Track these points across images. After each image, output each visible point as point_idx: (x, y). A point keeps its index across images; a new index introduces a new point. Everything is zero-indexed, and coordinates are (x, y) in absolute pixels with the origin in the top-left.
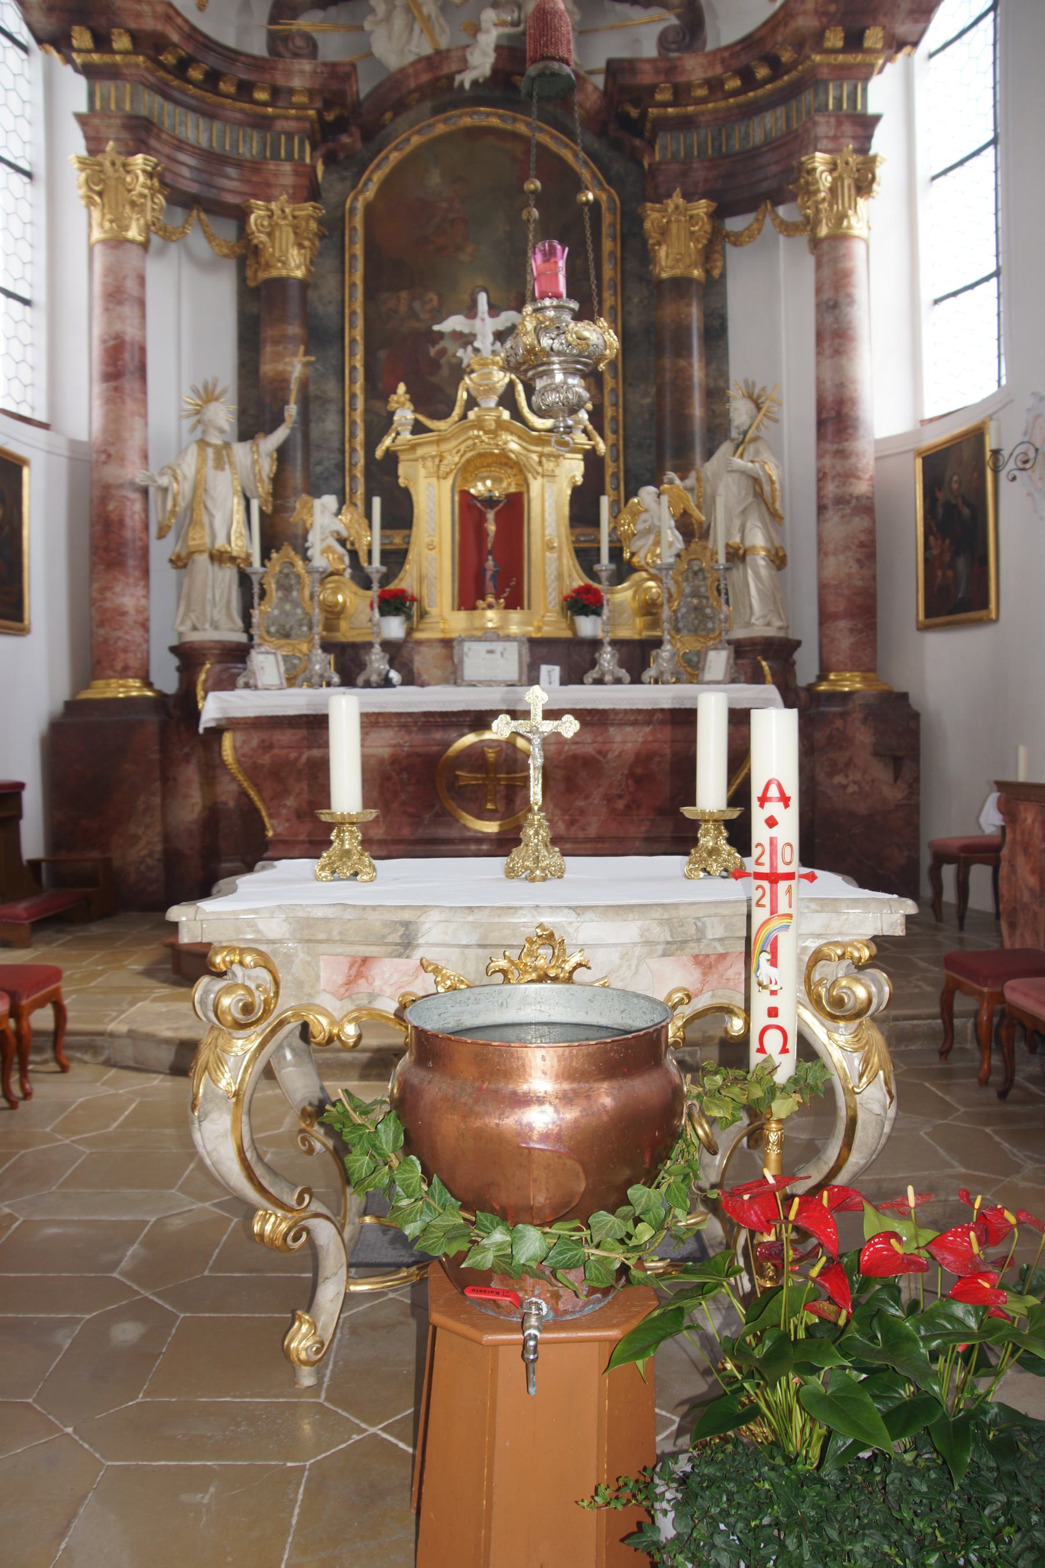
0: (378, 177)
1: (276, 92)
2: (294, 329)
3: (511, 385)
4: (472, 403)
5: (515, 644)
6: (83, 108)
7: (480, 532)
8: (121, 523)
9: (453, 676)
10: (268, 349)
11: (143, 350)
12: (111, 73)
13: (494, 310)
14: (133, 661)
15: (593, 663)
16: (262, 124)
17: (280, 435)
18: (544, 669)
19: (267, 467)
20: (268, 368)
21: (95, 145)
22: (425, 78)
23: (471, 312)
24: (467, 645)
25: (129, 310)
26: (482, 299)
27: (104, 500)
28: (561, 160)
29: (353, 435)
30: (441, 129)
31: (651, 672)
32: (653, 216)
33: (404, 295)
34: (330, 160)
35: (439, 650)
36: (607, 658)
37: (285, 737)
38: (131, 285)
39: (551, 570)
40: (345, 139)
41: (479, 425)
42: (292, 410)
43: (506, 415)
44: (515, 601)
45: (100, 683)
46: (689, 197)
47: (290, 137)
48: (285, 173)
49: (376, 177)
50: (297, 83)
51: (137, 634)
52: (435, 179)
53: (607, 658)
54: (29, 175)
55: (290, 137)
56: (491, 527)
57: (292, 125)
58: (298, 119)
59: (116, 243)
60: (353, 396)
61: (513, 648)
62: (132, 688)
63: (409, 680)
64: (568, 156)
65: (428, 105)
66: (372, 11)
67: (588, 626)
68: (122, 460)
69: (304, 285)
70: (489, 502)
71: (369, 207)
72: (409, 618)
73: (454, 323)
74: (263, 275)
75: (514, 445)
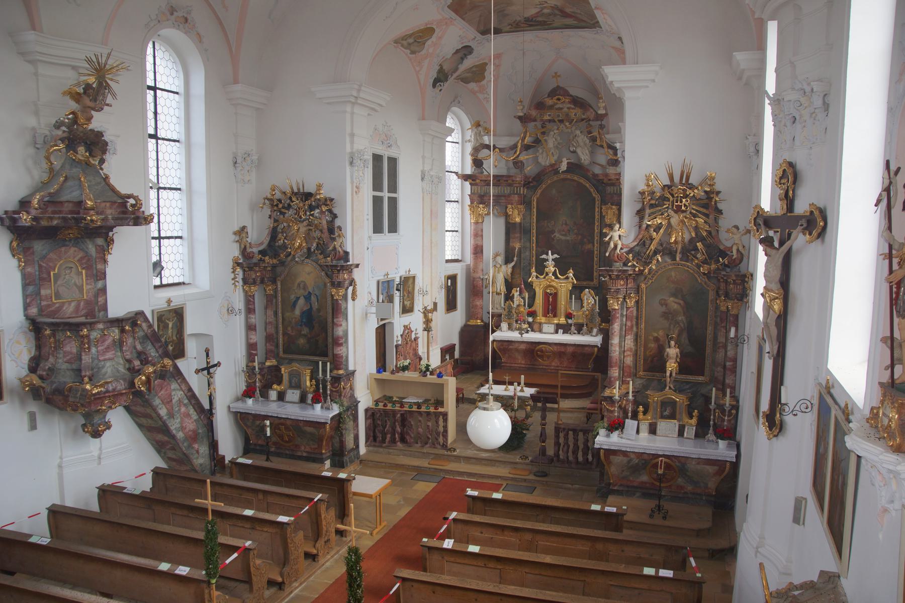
0: (540, 191)
1: (513, 181)
2: (518, 235)
3: (555, 270)
4: (547, 274)
5: (553, 325)
6: (469, 203)
7: (549, 300)
8: (477, 286)
9: (540, 331)
10: (511, 240)
11: (482, 246)
12: (476, 184)
13: (552, 255)
14: (479, 316)
15: (570, 329)
16: (510, 185)
17: (513, 264)
18: (559, 330)
19: (510, 271)
20: (511, 244)
21: (472, 202)
22: (550, 169)
23: (547, 254)
24: (544, 325)
25: (479, 238)
26: (550, 252)
27: (474, 281)
28: (586, 186)
29: (533, 257)
30: (555, 178)
31: (581, 332)
32: (604, 207)
33: (546, 221)
34: (527, 188)
35: (538, 325)
36: (573, 328)
37: (505, 344)
38: (480, 233)
39: (562, 310)
40: (531, 184)
41: (547, 280)
42: (515, 259)
43: (553, 277)
44: (555, 316)
45: (472, 321)
46: (612, 204)
47: (517, 187)
48: (516, 198)
49: (539, 191)
50: (518, 179)
51: (480, 310)
52: (554, 191)
53: (573, 328)
54: (457, 202)
55: (517, 187)
56: (551, 300)
57: (518, 185)
58: (519, 184)
59: (477, 223)
60: (533, 247)
61: (553, 325)
62: (479, 322)
63: (532, 331)
64: (587, 185)
65: (553, 172)
66: (538, 151)
67: (570, 321)
68: (477, 272)
69: (520, 223)
70: (551, 294)
71: (537, 199)
72: (533, 317)
73: (544, 256)
74: (511, 221)
75: (554, 284)
